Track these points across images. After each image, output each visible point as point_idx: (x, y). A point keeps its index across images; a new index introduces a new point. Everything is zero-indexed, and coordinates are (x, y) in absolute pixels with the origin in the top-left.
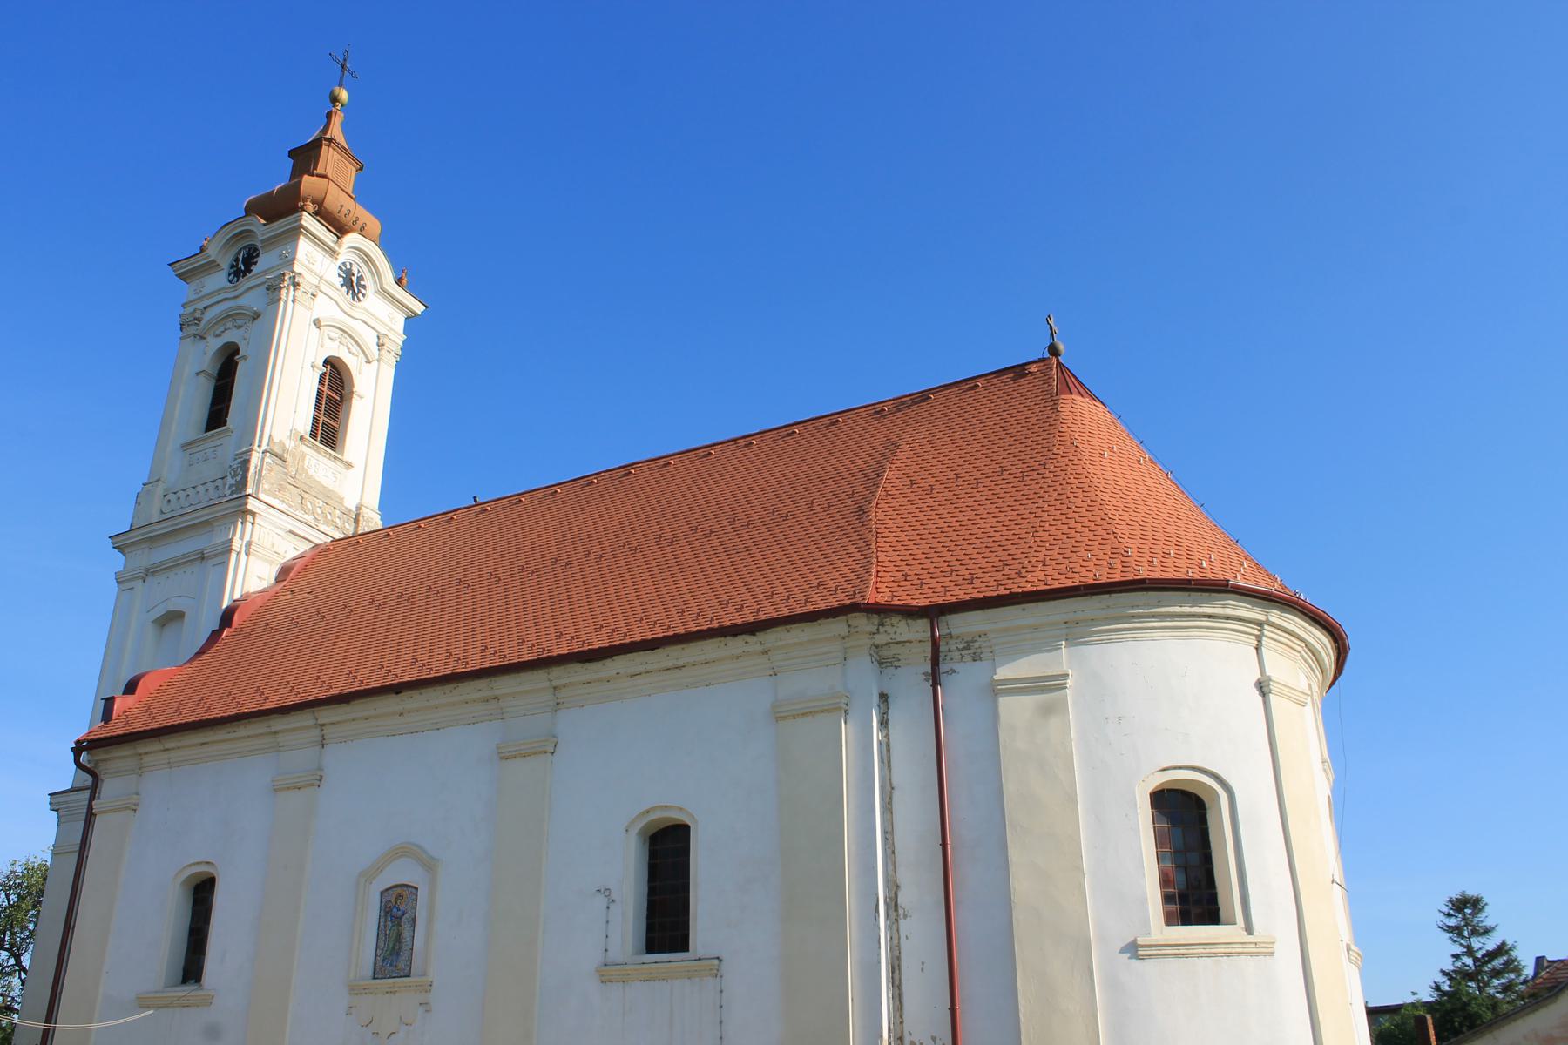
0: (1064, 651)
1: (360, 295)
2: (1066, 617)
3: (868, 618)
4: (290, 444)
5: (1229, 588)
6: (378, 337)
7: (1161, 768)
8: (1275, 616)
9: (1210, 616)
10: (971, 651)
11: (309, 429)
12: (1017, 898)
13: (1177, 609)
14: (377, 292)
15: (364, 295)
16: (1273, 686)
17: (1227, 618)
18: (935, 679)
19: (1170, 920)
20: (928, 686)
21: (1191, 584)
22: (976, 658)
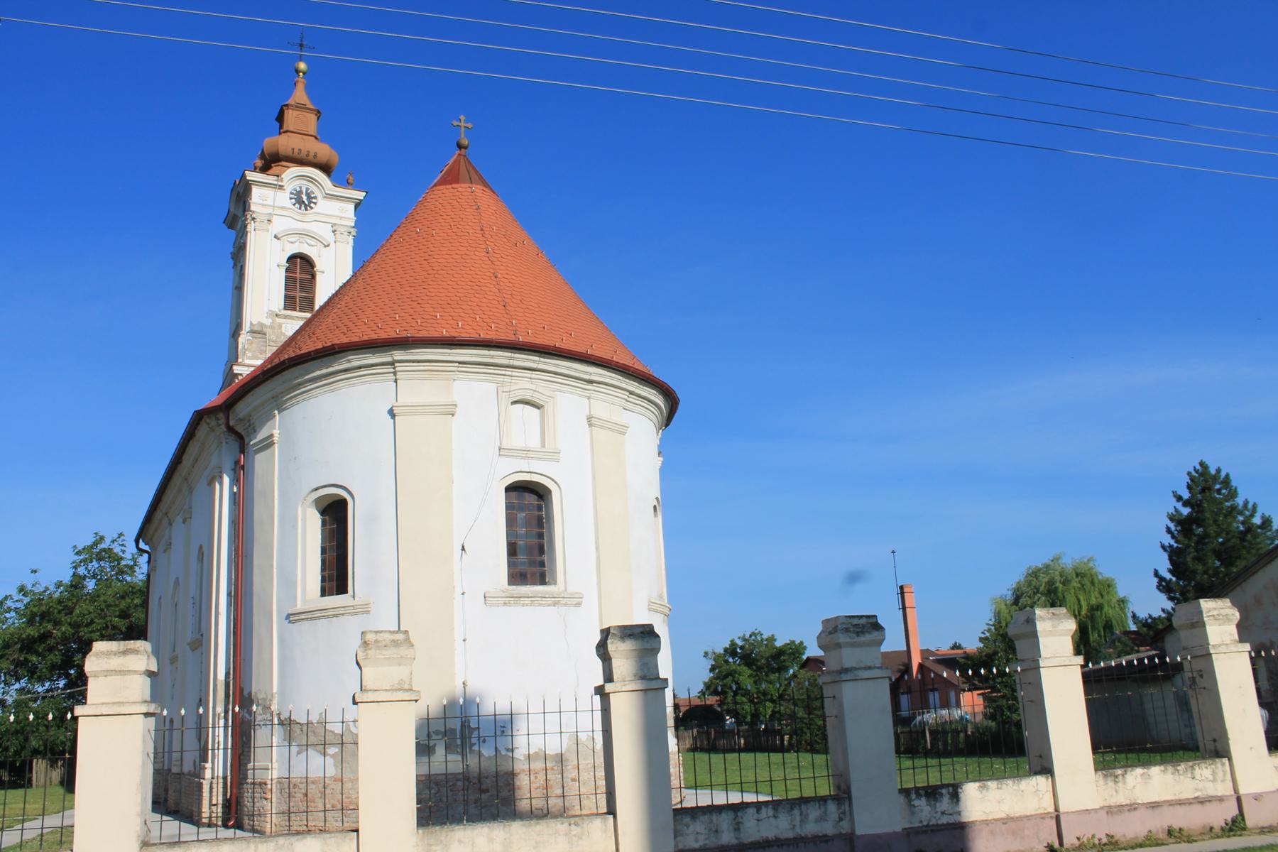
1: (312, 205)
4: (267, 322)
5: (337, 350)
6: (332, 227)
7: (310, 490)
9: (345, 371)
11: (282, 306)
14: (325, 197)
15: (315, 203)
17: (360, 367)
21: (311, 355)
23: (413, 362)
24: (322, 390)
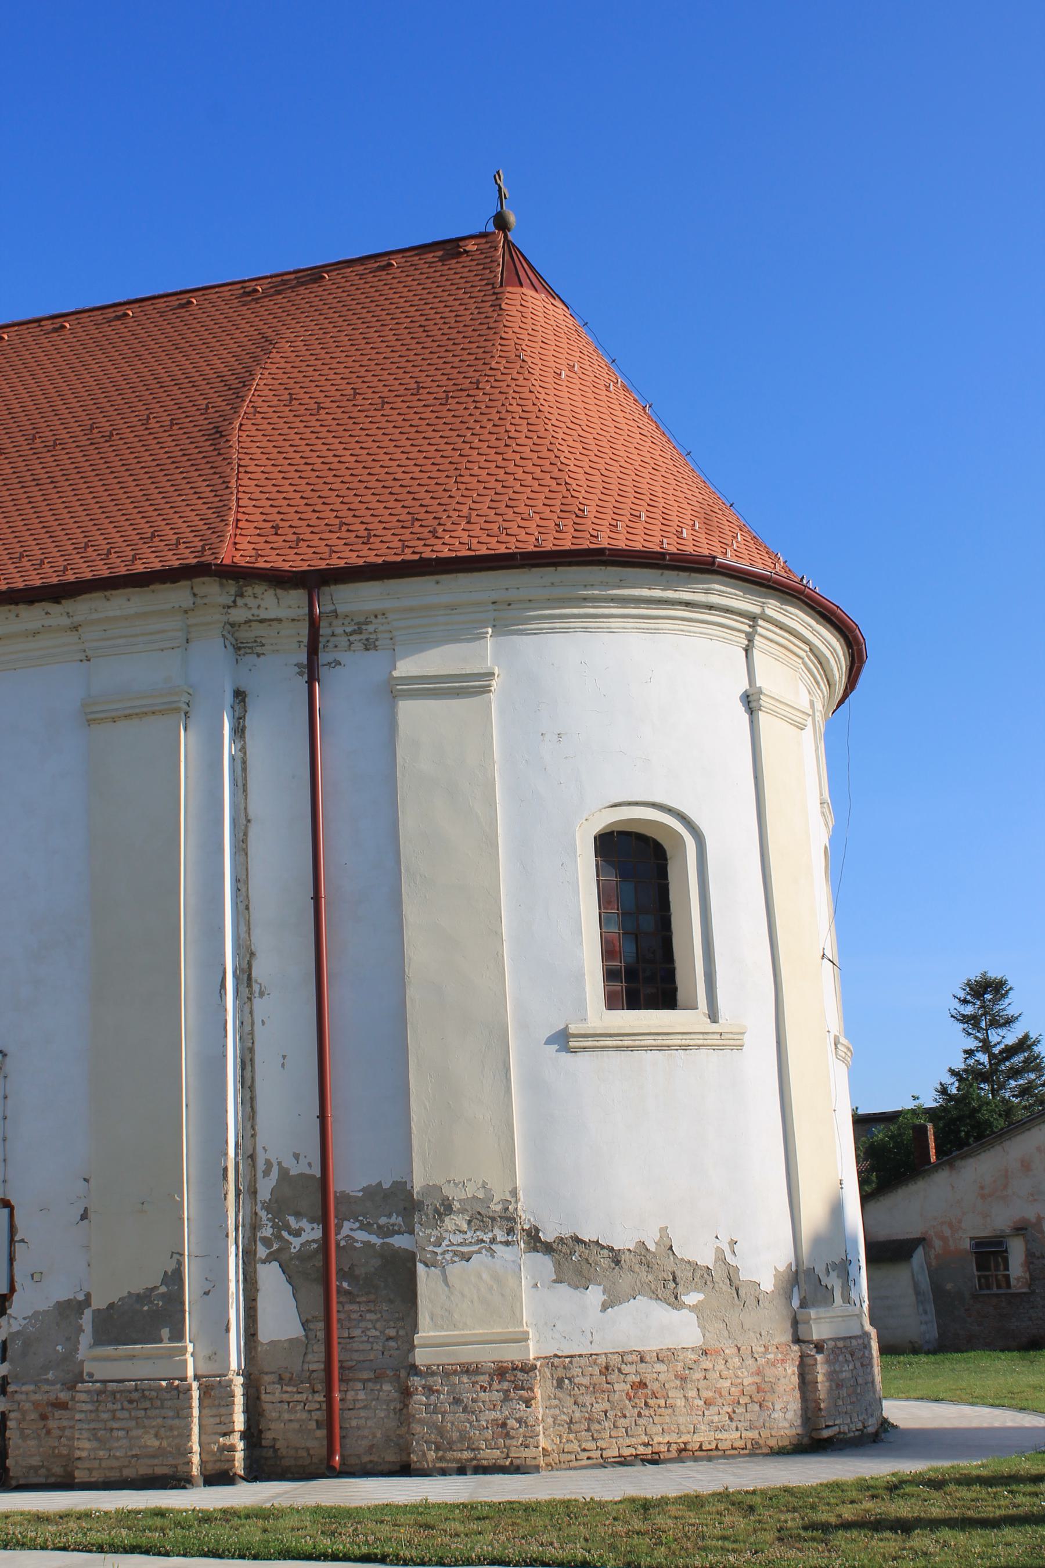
0: (489, 642)
2: (495, 596)
3: (222, 585)
5: (715, 568)
8: (773, 608)
9: (688, 604)
10: (364, 636)
12: (411, 971)
13: (645, 592)
16: (764, 701)
17: (711, 607)
18: (312, 672)
19: (612, 1002)
20: (302, 682)
21: (664, 559)
22: (369, 646)
23: (781, 628)
24: (631, 623)
